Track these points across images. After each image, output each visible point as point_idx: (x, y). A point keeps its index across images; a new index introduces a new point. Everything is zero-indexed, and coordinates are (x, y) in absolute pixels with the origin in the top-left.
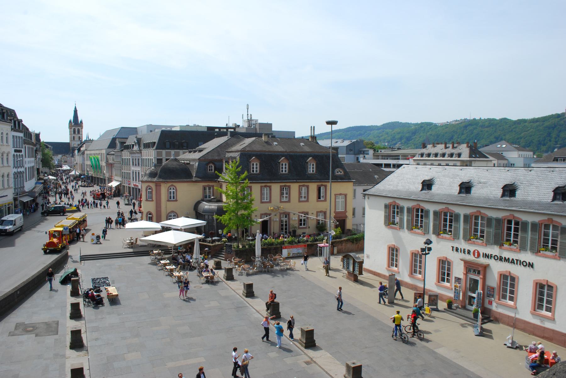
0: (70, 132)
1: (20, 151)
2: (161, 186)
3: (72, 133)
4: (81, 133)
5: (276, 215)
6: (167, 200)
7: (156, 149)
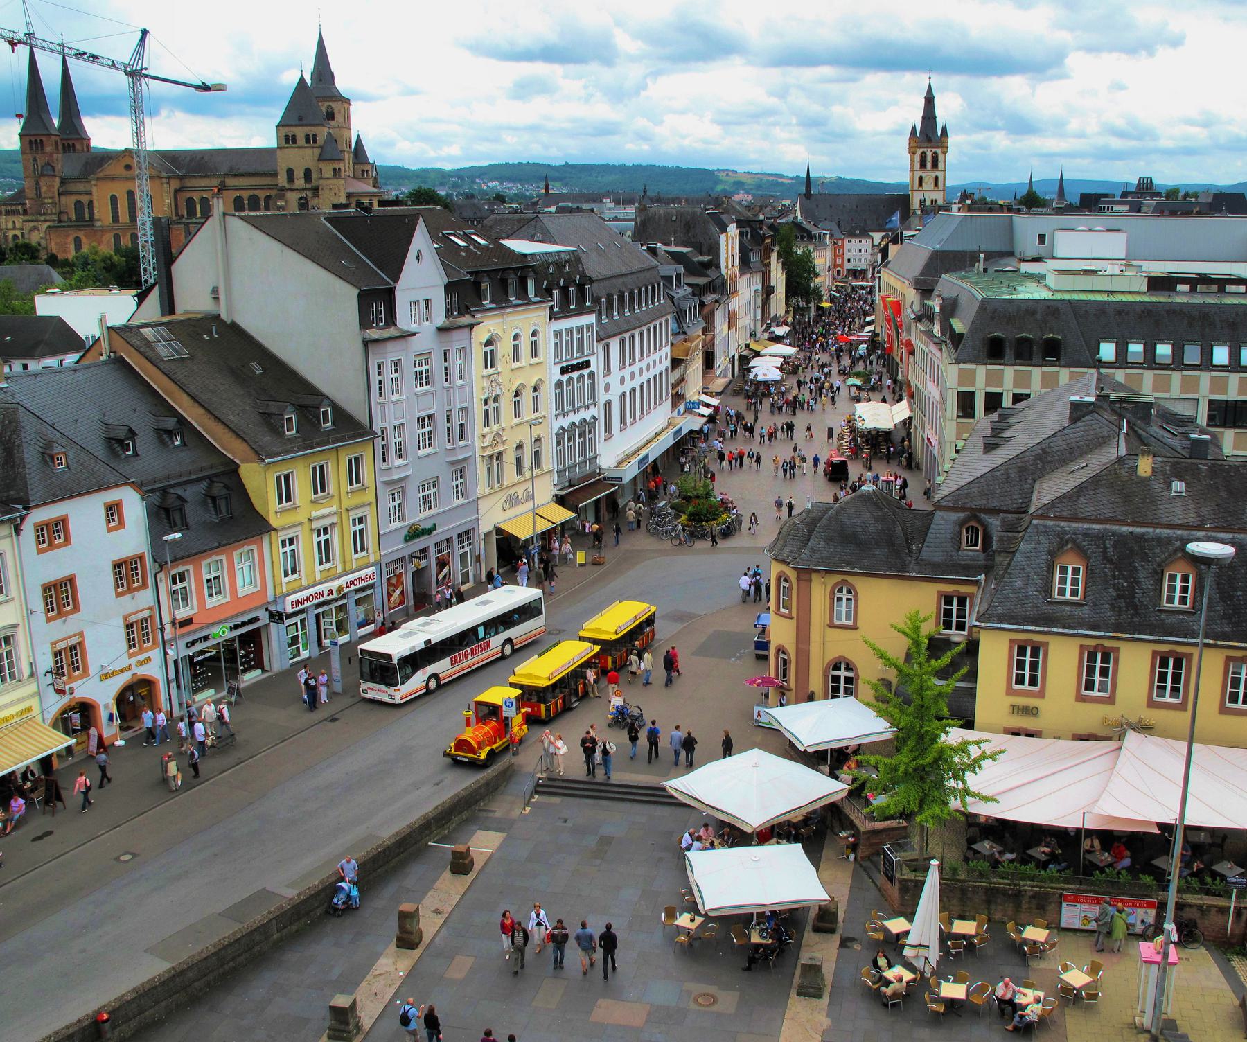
0: (912, 162)
2: (810, 580)
3: (917, 165)
6: (827, 622)
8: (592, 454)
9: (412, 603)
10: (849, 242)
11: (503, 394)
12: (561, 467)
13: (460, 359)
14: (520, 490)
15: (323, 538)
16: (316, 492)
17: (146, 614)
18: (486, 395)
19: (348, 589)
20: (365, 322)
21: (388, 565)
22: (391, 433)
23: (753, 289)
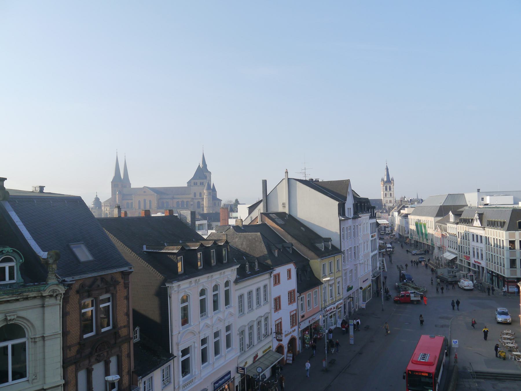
3: (385, 190)
4: (392, 190)
7: (508, 230)
9: (348, 314)
17: (295, 312)
20: (340, 214)
22: (346, 252)
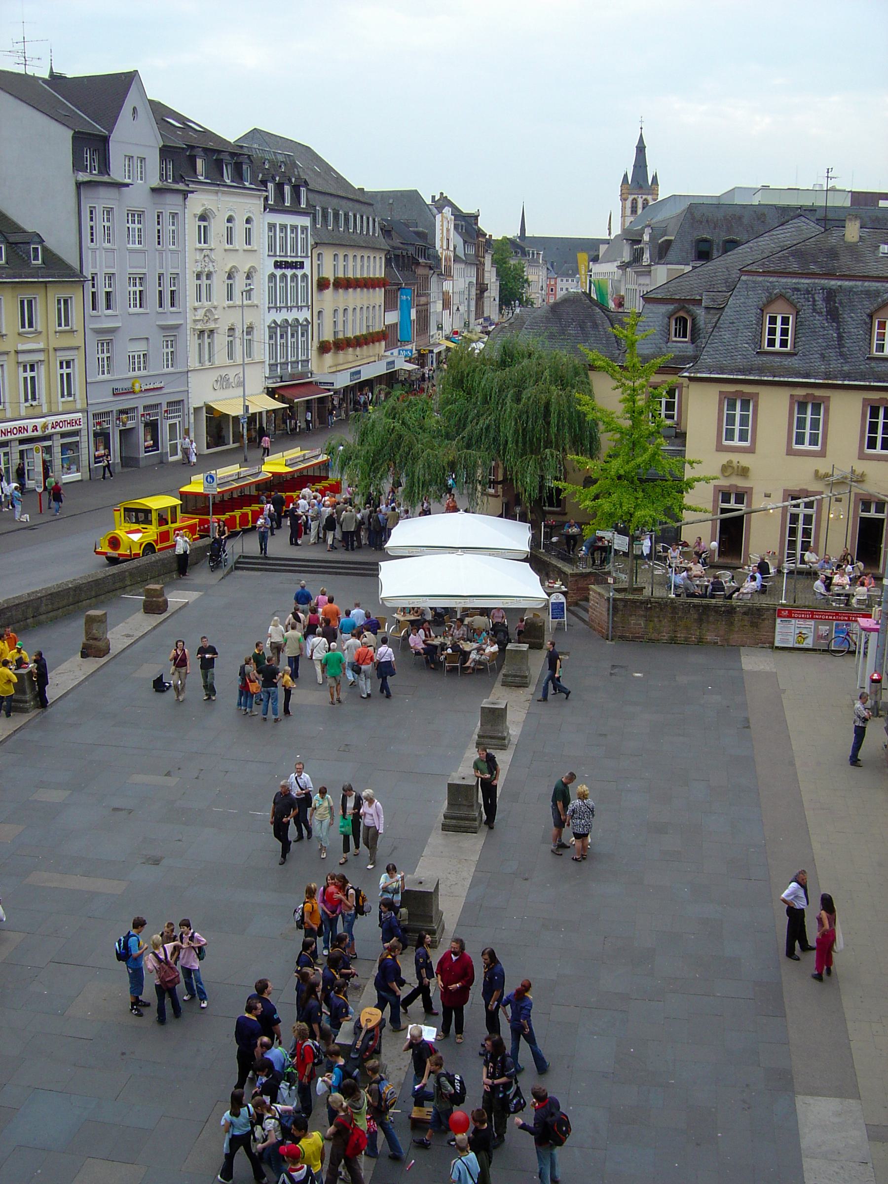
0: (624, 208)
1: (301, 265)
5: (839, 500)
8: (304, 358)
10: (562, 280)
11: (215, 272)
12: (272, 362)
13: (173, 224)
14: (232, 373)
15: (29, 374)
16: (23, 326)
18: (199, 270)
19: (53, 430)
20: (78, 165)
21: (95, 416)
22: (100, 281)
23: (468, 280)
